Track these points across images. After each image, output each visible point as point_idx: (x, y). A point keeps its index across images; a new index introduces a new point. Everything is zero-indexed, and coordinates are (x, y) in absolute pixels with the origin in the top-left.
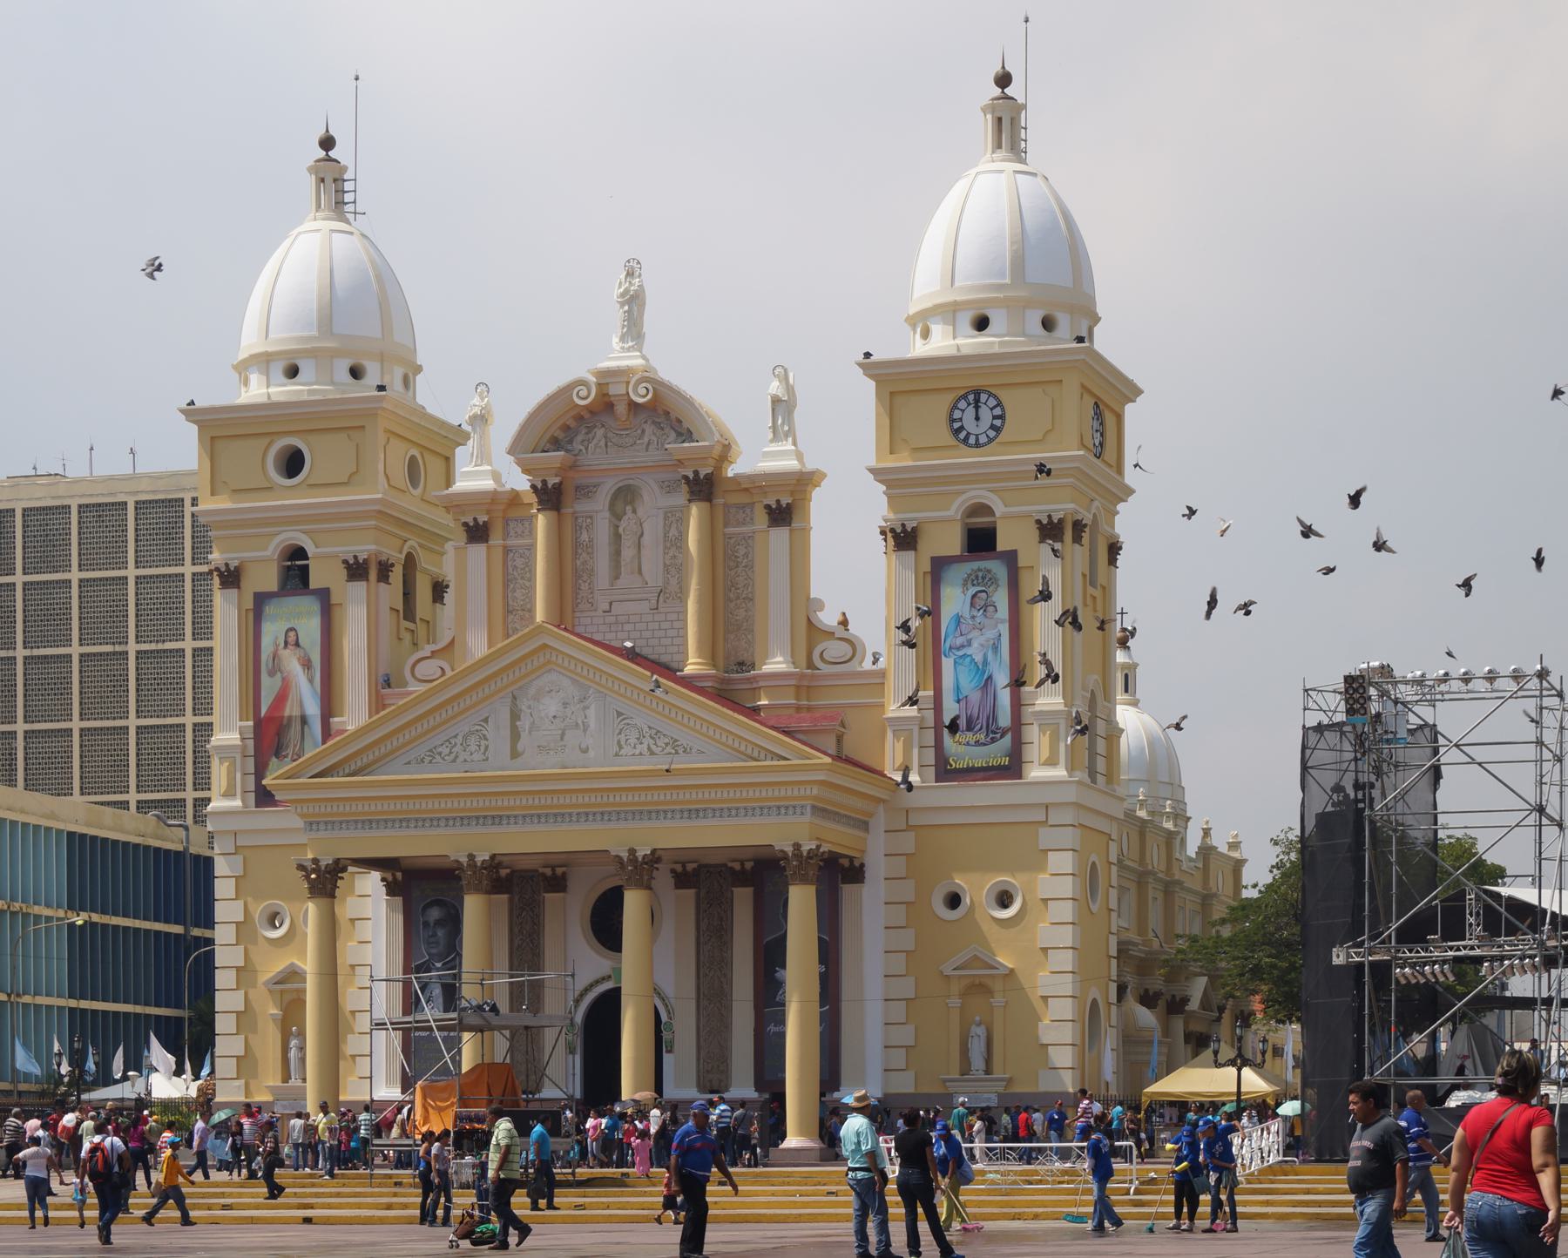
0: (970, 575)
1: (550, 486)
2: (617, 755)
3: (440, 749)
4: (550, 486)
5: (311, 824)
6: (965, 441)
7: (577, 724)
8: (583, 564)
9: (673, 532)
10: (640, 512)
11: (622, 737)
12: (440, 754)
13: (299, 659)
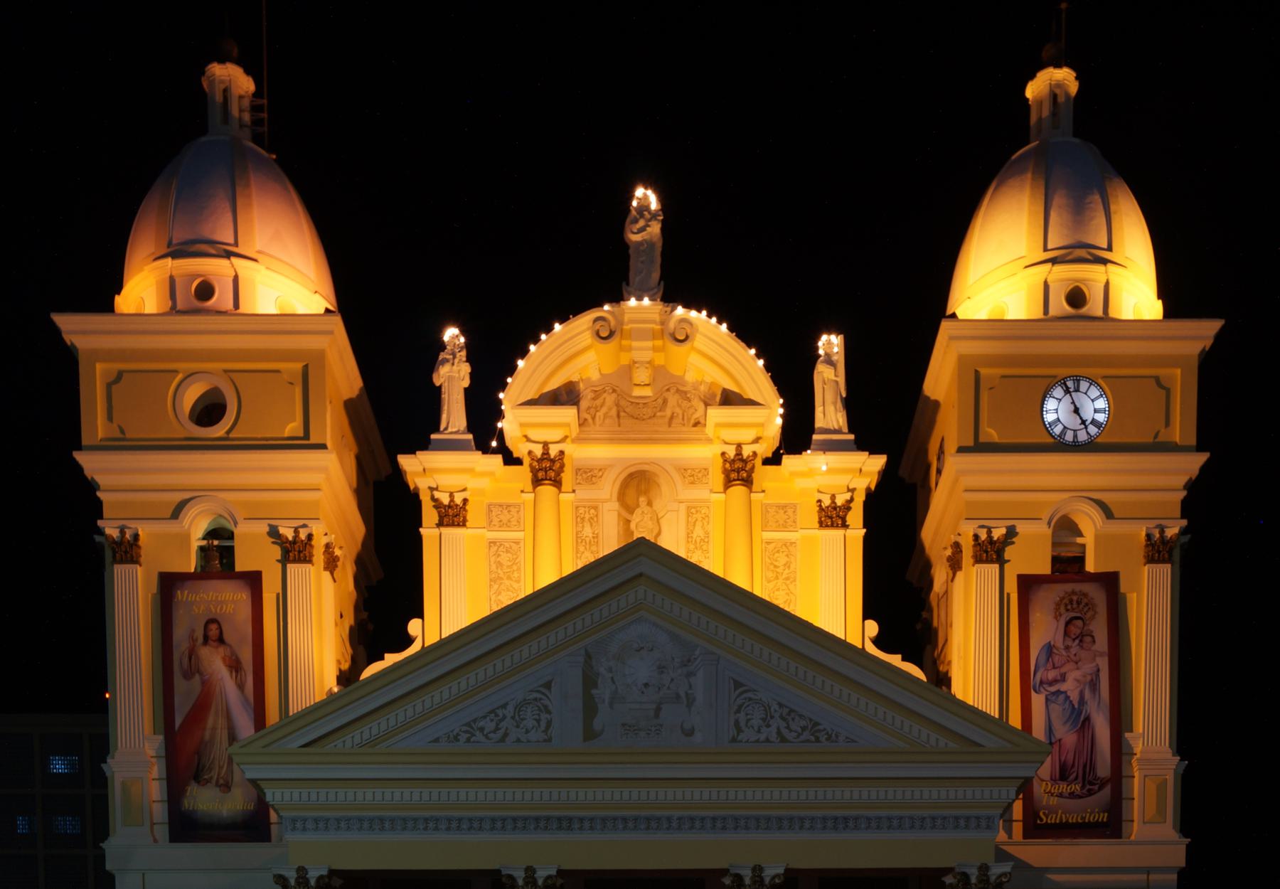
0: (1063, 598)
2: (734, 740)
3: (481, 724)
7: (678, 696)
9: (698, 532)
10: (657, 505)
11: (742, 717)
12: (482, 729)
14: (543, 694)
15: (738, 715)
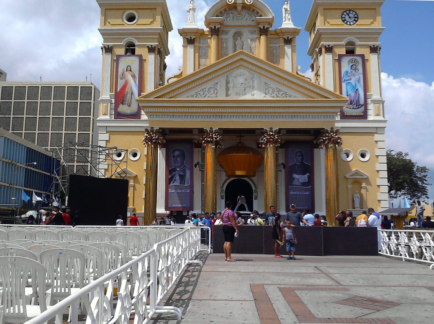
1: (216, 28)
3: (200, 93)
4: (216, 28)
5: (151, 116)
6: (346, 23)
7: (250, 86)
8: (224, 53)
10: (243, 39)
12: (200, 94)
13: (131, 75)
14: (216, 86)
15: (266, 91)
